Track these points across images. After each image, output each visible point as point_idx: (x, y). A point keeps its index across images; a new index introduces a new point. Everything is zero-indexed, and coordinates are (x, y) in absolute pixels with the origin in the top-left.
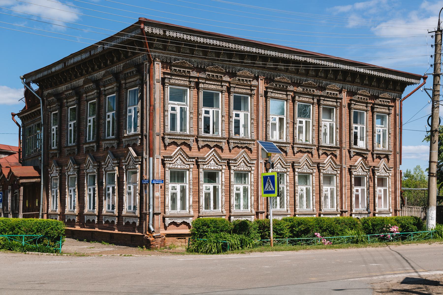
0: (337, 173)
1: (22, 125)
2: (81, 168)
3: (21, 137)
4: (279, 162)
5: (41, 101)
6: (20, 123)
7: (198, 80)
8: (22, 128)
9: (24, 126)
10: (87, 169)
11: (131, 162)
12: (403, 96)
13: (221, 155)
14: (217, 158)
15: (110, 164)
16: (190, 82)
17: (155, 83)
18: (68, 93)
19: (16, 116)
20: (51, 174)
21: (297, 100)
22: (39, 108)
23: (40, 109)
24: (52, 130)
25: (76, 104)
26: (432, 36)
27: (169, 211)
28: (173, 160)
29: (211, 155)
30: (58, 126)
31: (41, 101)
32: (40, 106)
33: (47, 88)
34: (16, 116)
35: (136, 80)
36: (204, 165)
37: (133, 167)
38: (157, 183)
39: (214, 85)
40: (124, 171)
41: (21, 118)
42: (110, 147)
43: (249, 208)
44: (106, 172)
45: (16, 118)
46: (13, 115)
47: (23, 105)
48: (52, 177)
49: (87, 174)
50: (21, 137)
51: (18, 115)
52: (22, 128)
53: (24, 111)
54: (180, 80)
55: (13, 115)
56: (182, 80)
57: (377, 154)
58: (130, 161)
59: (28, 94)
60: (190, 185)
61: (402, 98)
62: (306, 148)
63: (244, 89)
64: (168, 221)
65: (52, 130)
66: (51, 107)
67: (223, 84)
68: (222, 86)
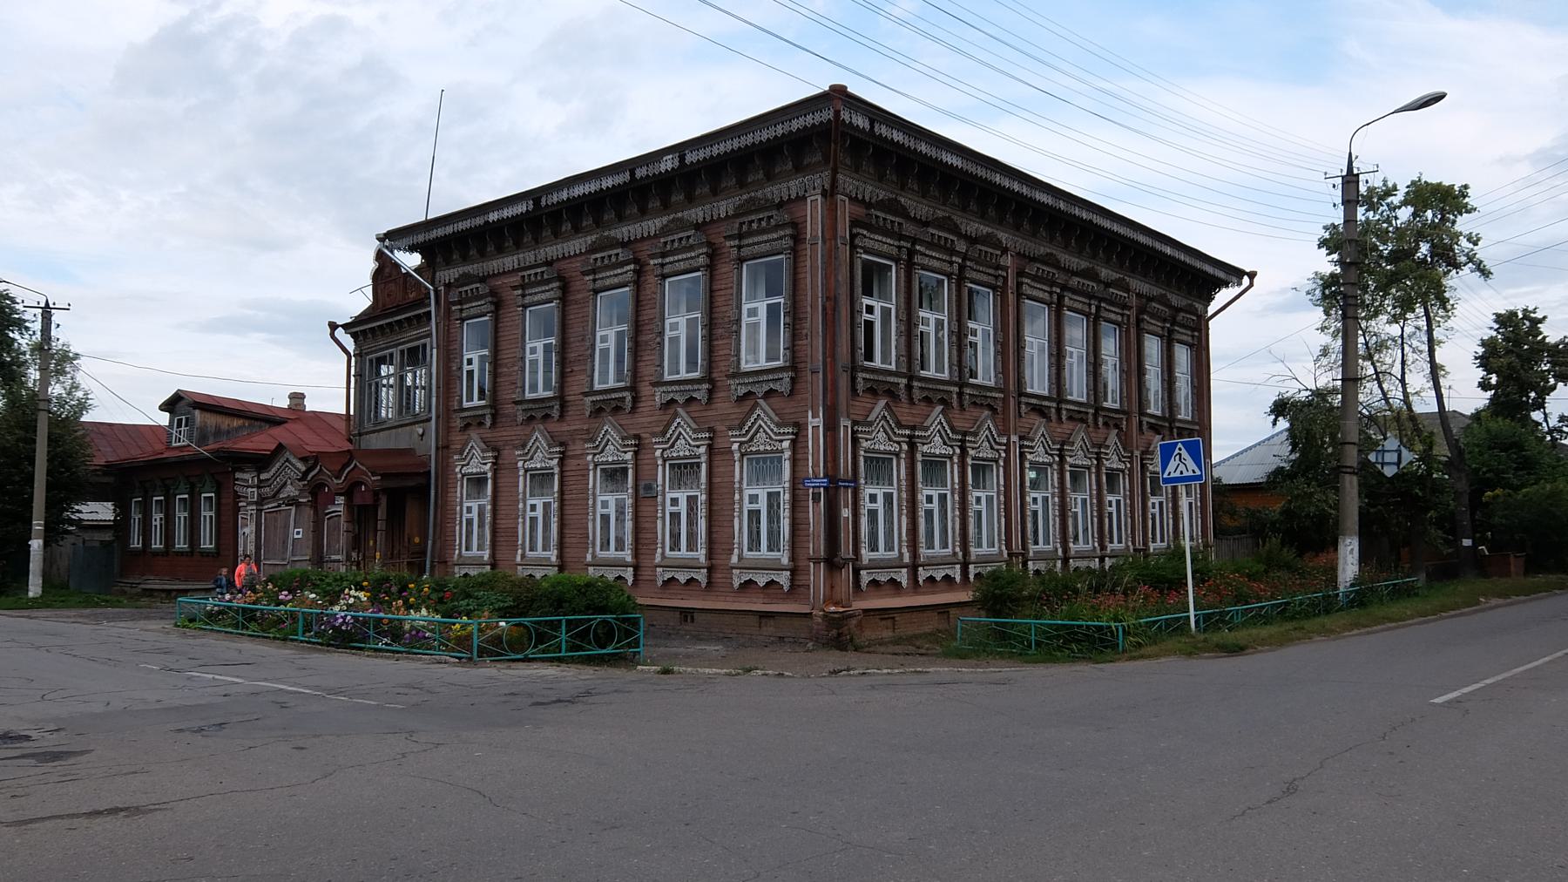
0: (1126, 467)
1: (354, 351)
2: (567, 454)
3: (353, 379)
4: (1042, 442)
5: (432, 293)
6: (351, 347)
7: (913, 244)
8: (353, 359)
9: (359, 355)
10: (595, 455)
11: (761, 434)
12: (1211, 310)
13: (955, 424)
14: (947, 428)
15: (683, 441)
16: (899, 248)
17: (839, 245)
18: (533, 272)
19: (340, 328)
20: (463, 466)
21: (1067, 307)
22: (428, 309)
23: (430, 311)
24: (465, 362)
25: (556, 299)
26: (1334, 186)
27: (866, 555)
28: (872, 431)
29: (936, 422)
30: (490, 352)
31: (432, 293)
32: (430, 305)
33: (448, 263)
34: (340, 328)
35: (781, 238)
36: (924, 444)
37: (768, 448)
38: (844, 486)
39: (938, 259)
40: (736, 458)
41: (354, 336)
42: (681, 399)
43: (996, 545)
44: (665, 461)
45: (340, 333)
46: (333, 326)
47: (362, 301)
48: (463, 475)
49: (596, 466)
50: (353, 379)
51: (345, 327)
52: (353, 359)
53: (358, 321)
54: (881, 241)
55: (333, 326)
56: (886, 243)
57: (1178, 428)
58: (757, 432)
59: (385, 272)
60: (899, 491)
61: (1209, 314)
62: (1080, 412)
63: (985, 273)
64: (865, 577)
65: (465, 362)
66: (465, 307)
67: (954, 259)
68: (951, 263)
